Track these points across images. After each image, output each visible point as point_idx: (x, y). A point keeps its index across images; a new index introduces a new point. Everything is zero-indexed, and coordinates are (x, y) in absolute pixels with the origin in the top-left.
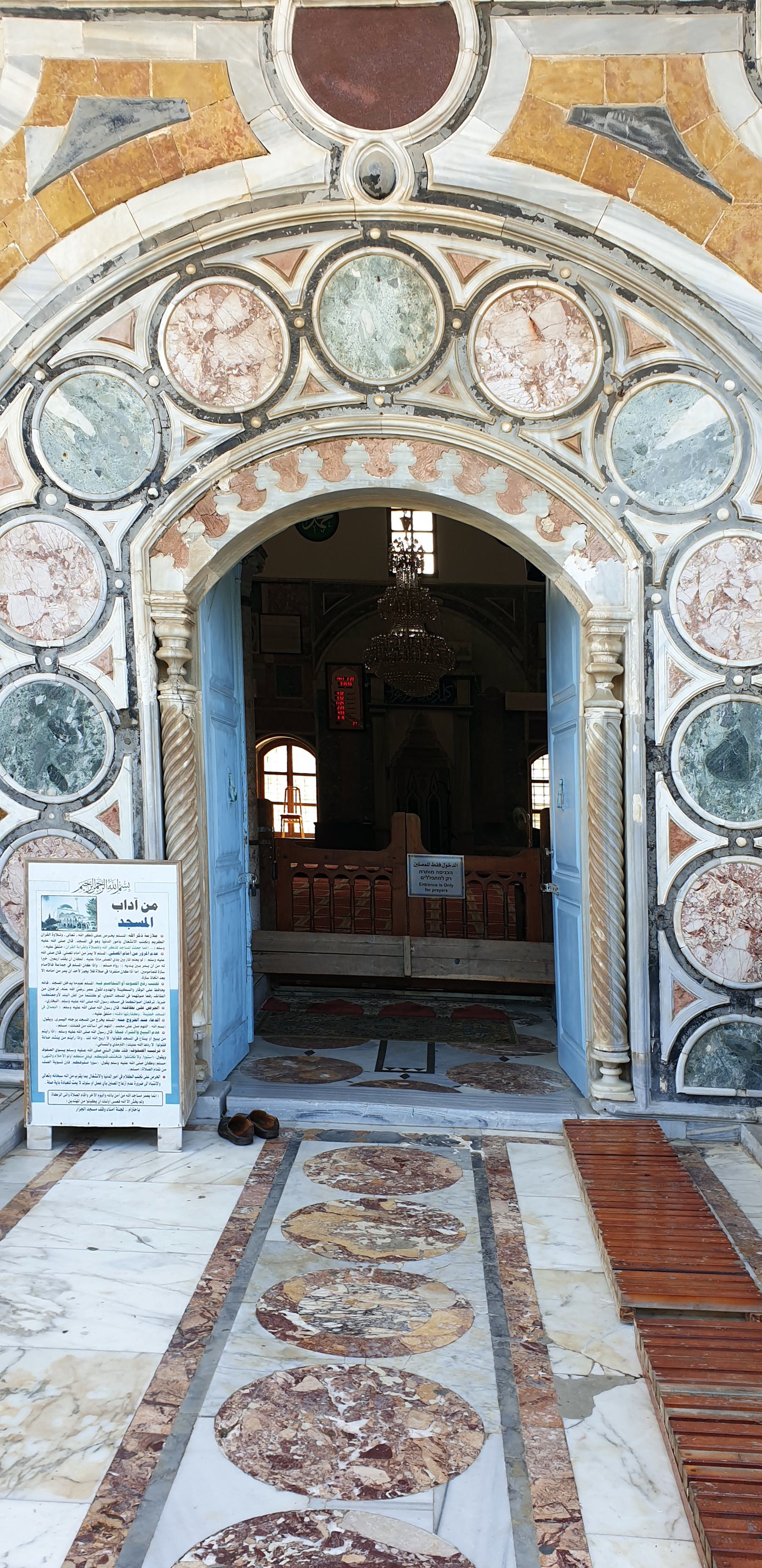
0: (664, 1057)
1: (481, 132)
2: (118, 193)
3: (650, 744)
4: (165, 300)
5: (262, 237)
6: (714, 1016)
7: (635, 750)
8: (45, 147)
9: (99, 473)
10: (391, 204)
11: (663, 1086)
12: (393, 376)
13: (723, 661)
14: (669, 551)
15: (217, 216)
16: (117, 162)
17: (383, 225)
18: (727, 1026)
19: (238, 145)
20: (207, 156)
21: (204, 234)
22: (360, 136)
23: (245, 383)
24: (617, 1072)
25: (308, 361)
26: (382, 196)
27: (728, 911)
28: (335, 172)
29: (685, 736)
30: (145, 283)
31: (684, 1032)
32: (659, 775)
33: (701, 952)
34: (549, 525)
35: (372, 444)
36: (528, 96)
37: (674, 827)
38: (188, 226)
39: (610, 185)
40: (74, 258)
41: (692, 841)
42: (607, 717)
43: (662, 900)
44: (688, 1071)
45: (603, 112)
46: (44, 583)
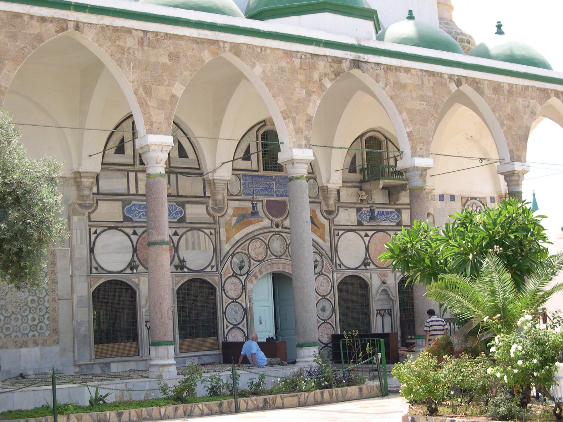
4: (250, 242)
12: (280, 254)
15: (256, 230)
17: (278, 232)
23: (260, 256)
40: (237, 236)
46: (234, 288)
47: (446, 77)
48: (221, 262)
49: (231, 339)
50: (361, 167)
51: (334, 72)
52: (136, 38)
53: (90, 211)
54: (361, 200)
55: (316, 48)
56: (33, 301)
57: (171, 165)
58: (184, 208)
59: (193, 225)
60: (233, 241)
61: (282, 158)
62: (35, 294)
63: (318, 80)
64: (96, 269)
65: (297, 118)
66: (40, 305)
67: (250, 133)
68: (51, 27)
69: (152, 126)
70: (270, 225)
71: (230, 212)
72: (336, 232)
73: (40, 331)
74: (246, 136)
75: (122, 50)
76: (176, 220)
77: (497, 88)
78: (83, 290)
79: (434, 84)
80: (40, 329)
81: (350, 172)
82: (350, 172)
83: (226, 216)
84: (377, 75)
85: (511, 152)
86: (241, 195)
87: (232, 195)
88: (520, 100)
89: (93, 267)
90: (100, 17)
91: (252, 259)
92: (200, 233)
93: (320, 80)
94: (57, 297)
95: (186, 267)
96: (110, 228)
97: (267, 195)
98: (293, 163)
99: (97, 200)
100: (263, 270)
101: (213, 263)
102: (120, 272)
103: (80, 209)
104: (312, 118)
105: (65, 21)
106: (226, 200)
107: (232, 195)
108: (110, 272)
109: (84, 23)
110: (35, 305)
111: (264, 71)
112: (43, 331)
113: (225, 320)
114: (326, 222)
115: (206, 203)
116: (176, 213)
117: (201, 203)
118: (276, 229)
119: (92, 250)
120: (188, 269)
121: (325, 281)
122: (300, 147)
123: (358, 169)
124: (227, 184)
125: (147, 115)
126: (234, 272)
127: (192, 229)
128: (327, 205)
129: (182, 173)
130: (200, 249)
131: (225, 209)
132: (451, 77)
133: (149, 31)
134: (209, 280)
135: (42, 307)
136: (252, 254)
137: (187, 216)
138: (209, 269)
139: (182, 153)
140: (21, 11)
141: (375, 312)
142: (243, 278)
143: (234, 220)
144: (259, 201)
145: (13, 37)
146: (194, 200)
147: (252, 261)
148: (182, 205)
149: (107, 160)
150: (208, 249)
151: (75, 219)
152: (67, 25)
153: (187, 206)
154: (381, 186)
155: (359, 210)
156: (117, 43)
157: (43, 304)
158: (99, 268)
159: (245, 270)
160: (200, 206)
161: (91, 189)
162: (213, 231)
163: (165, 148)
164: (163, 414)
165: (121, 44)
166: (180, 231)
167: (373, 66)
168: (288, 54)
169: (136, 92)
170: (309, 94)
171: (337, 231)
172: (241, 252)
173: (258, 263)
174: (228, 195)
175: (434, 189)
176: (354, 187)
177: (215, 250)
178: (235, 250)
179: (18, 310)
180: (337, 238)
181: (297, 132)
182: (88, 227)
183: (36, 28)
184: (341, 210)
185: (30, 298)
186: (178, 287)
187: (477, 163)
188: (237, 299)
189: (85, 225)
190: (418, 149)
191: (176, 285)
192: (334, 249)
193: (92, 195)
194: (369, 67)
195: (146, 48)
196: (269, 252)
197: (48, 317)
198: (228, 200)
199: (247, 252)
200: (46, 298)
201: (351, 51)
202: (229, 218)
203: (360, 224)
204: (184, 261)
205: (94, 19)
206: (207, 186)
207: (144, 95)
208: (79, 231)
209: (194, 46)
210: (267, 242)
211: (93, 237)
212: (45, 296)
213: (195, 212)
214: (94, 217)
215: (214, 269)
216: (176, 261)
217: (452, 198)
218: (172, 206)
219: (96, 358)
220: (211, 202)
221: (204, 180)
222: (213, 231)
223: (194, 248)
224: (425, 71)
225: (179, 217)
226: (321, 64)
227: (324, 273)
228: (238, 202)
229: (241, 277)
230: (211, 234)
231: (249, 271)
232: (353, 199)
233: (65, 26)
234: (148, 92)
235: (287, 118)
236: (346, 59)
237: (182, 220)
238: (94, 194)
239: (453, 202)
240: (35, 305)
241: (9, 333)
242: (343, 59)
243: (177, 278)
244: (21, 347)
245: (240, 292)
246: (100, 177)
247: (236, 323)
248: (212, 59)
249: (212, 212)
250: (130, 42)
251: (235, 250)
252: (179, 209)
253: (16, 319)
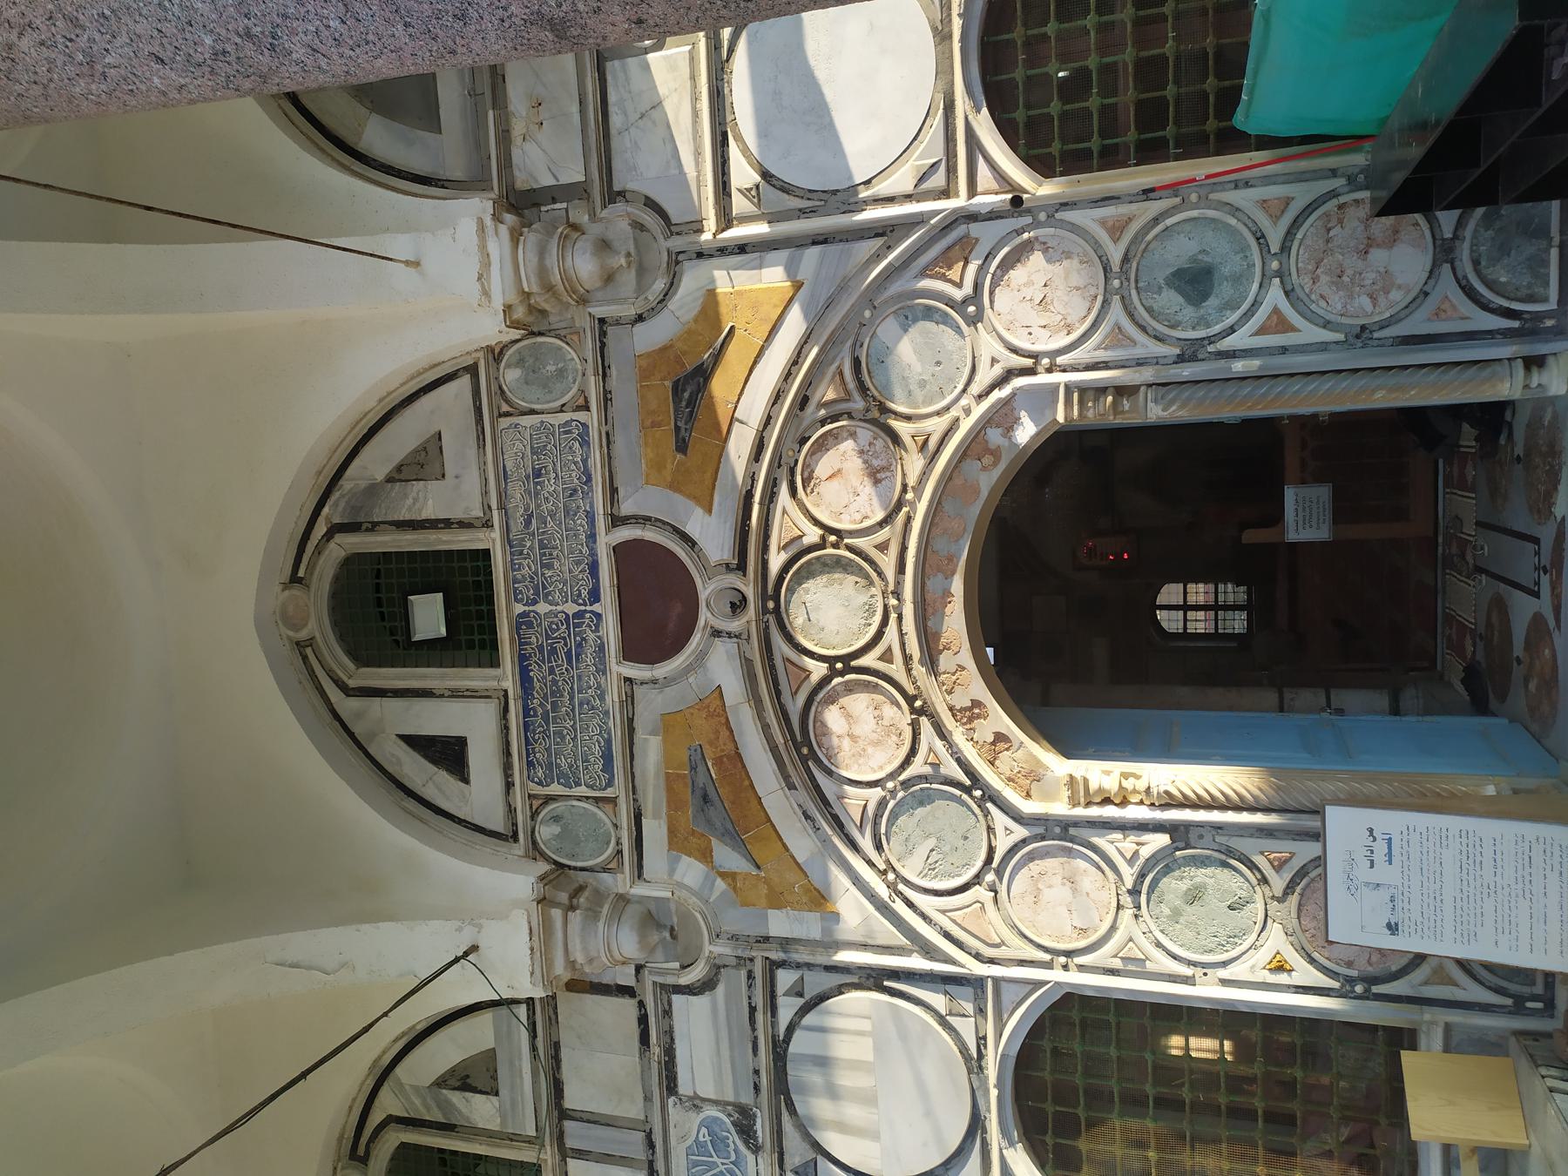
0: (1516, 324)
1: (697, 524)
2: (754, 802)
3: (1181, 359)
5: (778, 693)
6: (1465, 277)
7: (1187, 372)
8: (728, 857)
9: (966, 838)
10: (750, 592)
11: (1549, 323)
13: (1100, 298)
14: (1007, 352)
15: (766, 728)
16: (733, 803)
18: (1476, 263)
20: (724, 733)
21: (780, 740)
22: (704, 616)
24: (1535, 370)
25: (867, 660)
26: (744, 599)
27: (1349, 272)
28: (730, 635)
29: (1172, 327)
30: (817, 788)
31: (1485, 306)
32: (1211, 349)
33: (1395, 295)
34: (987, 460)
35: (930, 610)
36: (670, 488)
37: (1261, 331)
38: (774, 750)
41: (1276, 311)
42: (1156, 401)
43: (1340, 337)
44: (1531, 299)
45: (677, 428)
71: (691, 871)
118: (751, 611)
138: (966, 1028)
144: (629, 700)
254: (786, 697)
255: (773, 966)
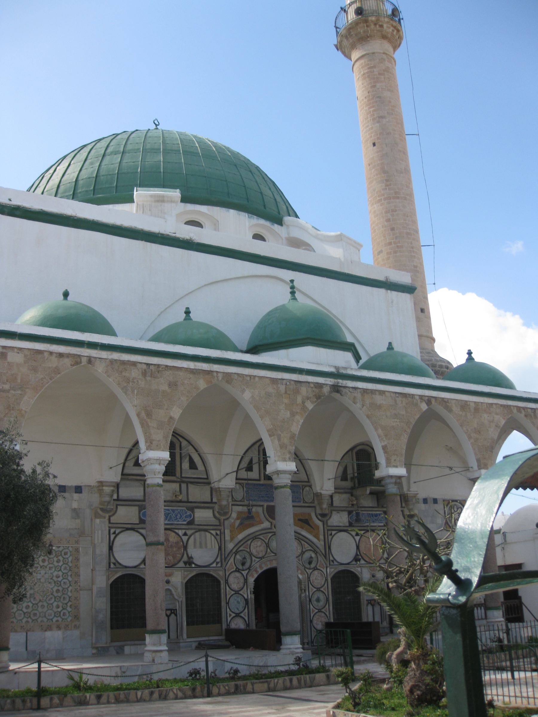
19: (261, 522)
38: (254, 533)
39: (302, 528)
40: (240, 537)
47: (417, 397)
48: (225, 559)
49: (233, 626)
50: (352, 475)
51: (315, 395)
52: (140, 370)
53: (110, 514)
54: (353, 505)
55: (300, 376)
56: (58, 591)
57: (183, 476)
58: (193, 512)
59: (201, 527)
60: (236, 540)
61: (270, 469)
62: (60, 585)
63: (301, 402)
64: (114, 564)
65: (282, 435)
66: (63, 594)
67: (253, 448)
68: (67, 362)
69: (151, 443)
70: (270, 526)
71: (234, 515)
72: (330, 532)
73: (63, 617)
74: (249, 451)
75: (128, 380)
76: (185, 523)
77: (464, 405)
78: (102, 582)
79: (407, 404)
80: (64, 615)
81: (342, 480)
82: (342, 480)
83: (230, 519)
84: (355, 398)
85: (478, 461)
86: (244, 501)
87: (236, 501)
88: (485, 416)
89: (112, 563)
90: (109, 353)
91: (254, 556)
92: (207, 533)
93: (303, 402)
94: (79, 588)
95: (194, 563)
96: (128, 529)
97: (267, 501)
98: (278, 474)
99: (117, 505)
100: (263, 565)
101: (218, 560)
102: (135, 567)
103: (100, 512)
104: (295, 435)
105: (79, 356)
106: (230, 505)
107: (236, 501)
108: (126, 567)
109: (96, 358)
110: (59, 594)
111: (253, 396)
112: (66, 617)
113: (228, 610)
114: (320, 524)
115: (212, 508)
116: (186, 517)
117: (208, 508)
119: (111, 548)
120: (195, 565)
121: (319, 575)
122: (284, 460)
123: (349, 477)
124: (232, 491)
125: (148, 434)
126: (237, 568)
127: (200, 530)
128: (321, 509)
129: (192, 483)
130: (206, 547)
131: (230, 513)
132: (421, 397)
133: (152, 364)
134: (214, 574)
135: (66, 596)
136: (254, 551)
137: (196, 519)
138: (214, 565)
139: (193, 465)
140: (43, 349)
141: (366, 602)
142: (245, 573)
143: (238, 522)
144: (260, 506)
145: (35, 370)
146: (203, 505)
147: (253, 558)
148: (192, 509)
149: (126, 471)
150: (213, 547)
151: (98, 521)
152: (81, 360)
153: (196, 510)
154: (368, 492)
155: (350, 513)
156: (124, 374)
157: (67, 594)
158: (117, 564)
159: (247, 565)
160: (207, 510)
161: (112, 496)
162: (218, 532)
163: (162, 462)
164: (139, 696)
165: (126, 374)
166: (189, 532)
167: (351, 390)
168: (274, 381)
169: (138, 415)
170: (293, 414)
171: (331, 531)
172: (244, 550)
173: (258, 560)
174: (232, 501)
175: (417, 494)
176: (346, 493)
177: (220, 548)
178: (238, 549)
179: (45, 598)
180: (330, 537)
181: (281, 447)
182: (108, 529)
183: (54, 362)
184: (334, 513)
185: (56, 588)
186: (186, 580)
187: (447, 471)
188: (240, 590)
189: (105, 526)
190: (392, 460)
191: (184, 578)
192: (328, 547)
193: (112, 501)
194: (347, 391)
195: (149, 378)
196: (269, 550)
197: (71, 605)
198: (232, 505)
199: (248, 550)
200: (70, 589)
201: (330, 378)
202: (233, 521)
203: (351, 525)
204: (192, 558)
205: (104, 354)
206: (214, 493)
207: (145, 417)
208: (100, 532)
209: (191, 376)
210: (267, 541)
211: (112, 537)
212: (68, 587)
213: (203, 515)
214: (113, 519)
215: (219, 565)
216: (185, 558)
217: (435, 501)
218: (182, 510)
219: (112, 641)
220: (217, 507)
221: (211, 488)
222: (218, 532)
223: (201, 547)
224: (398, 393)
225: (188, 519)
226: (304, 390)
227: (318, 568)
228: (241, 507)
229: (243, 572)
230: (217, 534)
231: (250, 566)
232: (344, 504)
233: (79, 360)
234: (149, 414)
235: (273, 435)
236: (327, 385)
237: (191, 523)
238: (114, 500)
239: (436, 505)
240: (59, 594)
241: (36, 618)
242: (324, 384)
243: (185, 573)
244: (46, 631)
245: (242, 585)
246: (120, 486)
247: (237, 612)
248: (206, 386)
249: (217, 515)
250: (135, 373)
251: (238, 549)
252: (189, 513)
253: (43, 606)
254: (263, 535)
255: (220, 530)
